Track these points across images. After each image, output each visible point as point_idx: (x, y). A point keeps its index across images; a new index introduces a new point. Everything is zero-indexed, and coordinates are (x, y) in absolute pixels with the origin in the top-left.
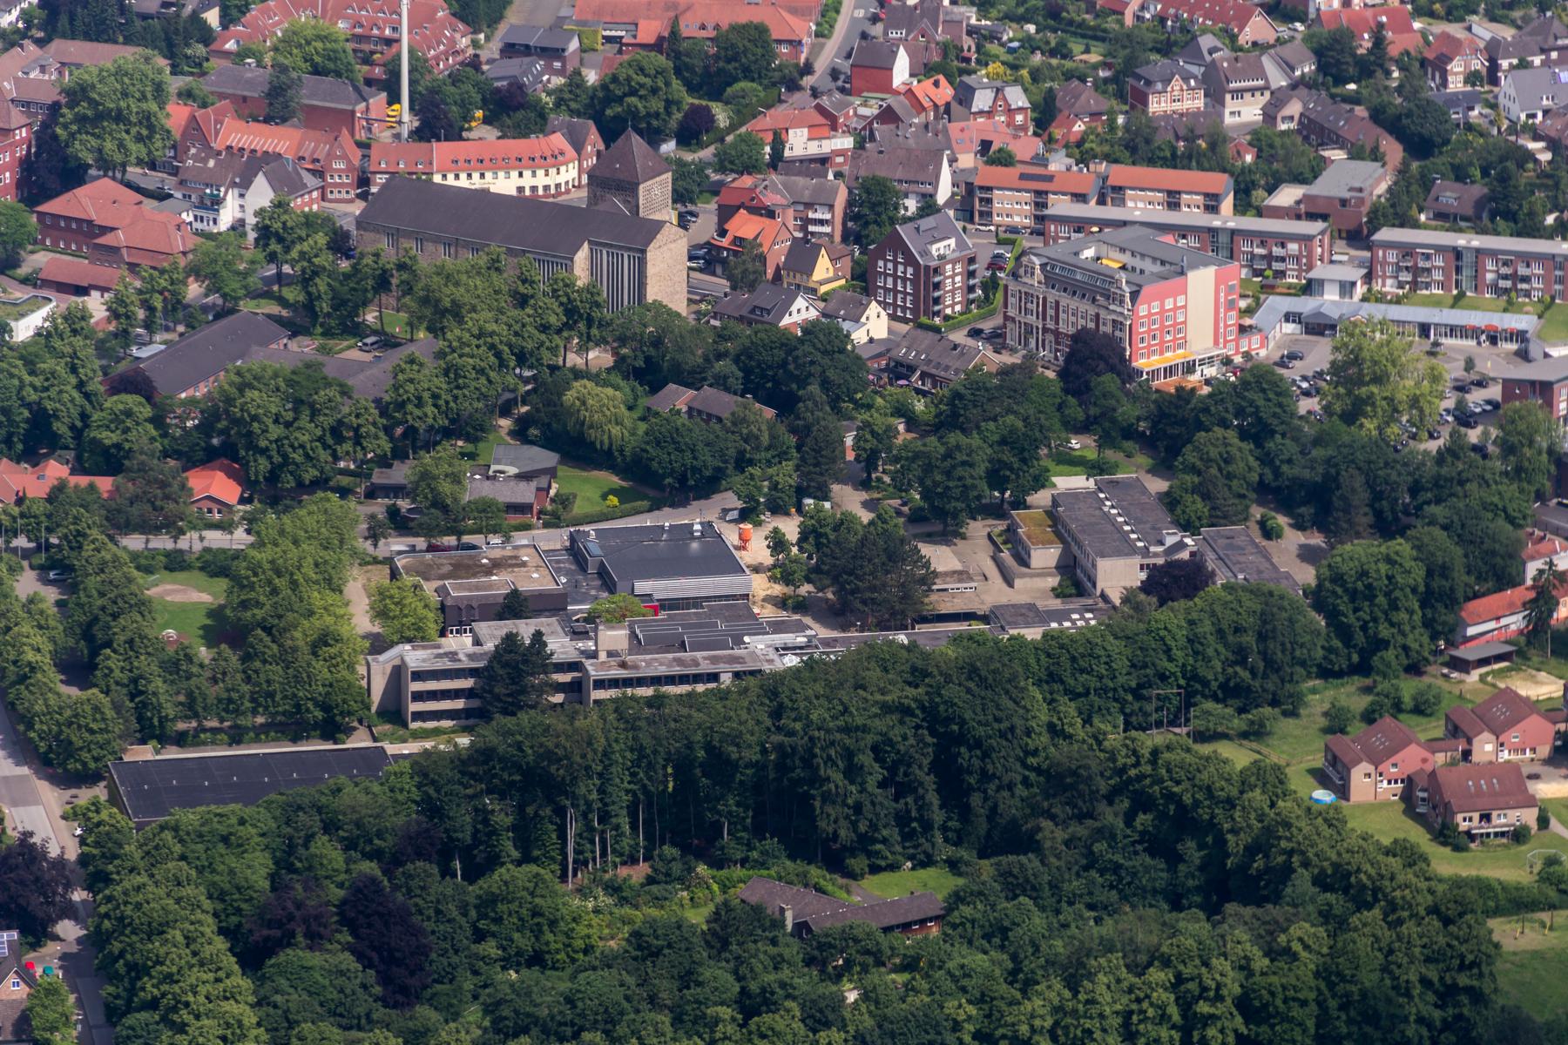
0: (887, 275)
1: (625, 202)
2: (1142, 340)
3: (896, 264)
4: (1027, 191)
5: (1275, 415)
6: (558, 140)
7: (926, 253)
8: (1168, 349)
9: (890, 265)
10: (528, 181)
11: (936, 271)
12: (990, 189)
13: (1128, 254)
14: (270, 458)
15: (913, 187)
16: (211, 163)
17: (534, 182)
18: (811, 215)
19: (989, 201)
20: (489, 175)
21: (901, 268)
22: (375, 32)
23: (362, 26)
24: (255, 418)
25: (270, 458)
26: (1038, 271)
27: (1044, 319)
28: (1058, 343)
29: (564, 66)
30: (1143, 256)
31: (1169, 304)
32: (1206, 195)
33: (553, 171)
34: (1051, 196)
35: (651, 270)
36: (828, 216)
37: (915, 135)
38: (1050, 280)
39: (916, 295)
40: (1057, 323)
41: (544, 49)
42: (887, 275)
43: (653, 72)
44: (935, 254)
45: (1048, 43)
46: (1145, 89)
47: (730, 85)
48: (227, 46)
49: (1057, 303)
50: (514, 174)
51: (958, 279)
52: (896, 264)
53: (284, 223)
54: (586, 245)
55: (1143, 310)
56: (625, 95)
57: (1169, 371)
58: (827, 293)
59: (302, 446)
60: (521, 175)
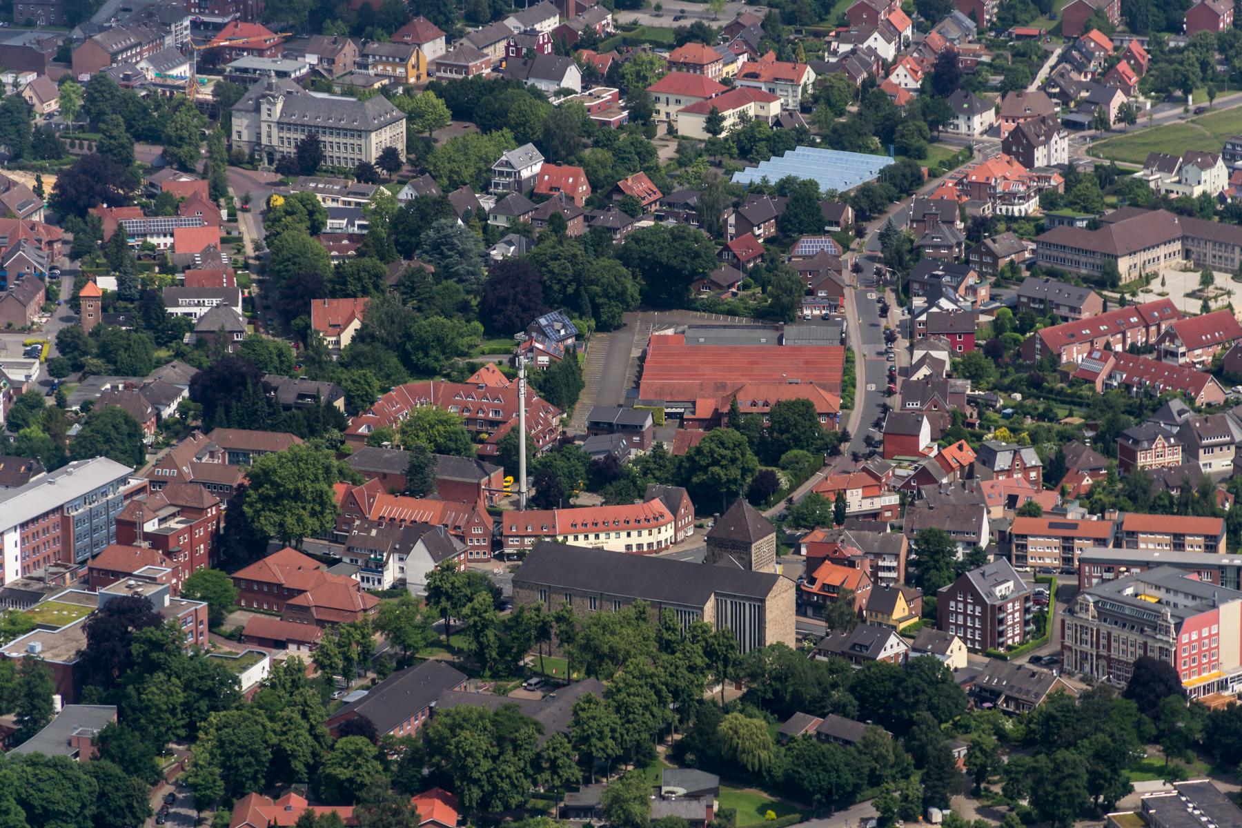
1: (740, 559)
3: (966, 604)
4: (1056, 538)
6: (657, 505)
7: (991, 594)
9: (961, 605)
10: (634, 540)
12: (1025, 537)
13: (1163, 591)
14: (481, 787)
15: (960, 537)
16: (374, 533)
17: (640, 540)
18: (880, 563)
19: (1024, 547)
20: (602, 536)
21: (970, 608)
22: (481, 415)
23: (469, 410)
24: (469, 754)
25: (481, 787)
26: (1092, 607)
27: (1098, 647)
28: (1109, 667)
29: (642, 440)
30: (1176, 592)
31: (1205, 633)
32: (1206, 537)
33: (655, 531)
35: (769, 616)
36: (895, 564)
37: (954, 492)
38: (1103, 615)
40: (1109, 650)
41: (624, 426)
43: (731, 445)
44: (998, 594)
45: (1036, 409)
46: (1133, 447)
47: (784, 452)
49: (1109, 634)
50: (623, 534)
51: (1017, 614)
52: (966, 604)
55: (1185, 639)
56: (708, 465)
57: (1207, 689)
58: (904, 629)
59: (509, 777)
60: (629, 535)
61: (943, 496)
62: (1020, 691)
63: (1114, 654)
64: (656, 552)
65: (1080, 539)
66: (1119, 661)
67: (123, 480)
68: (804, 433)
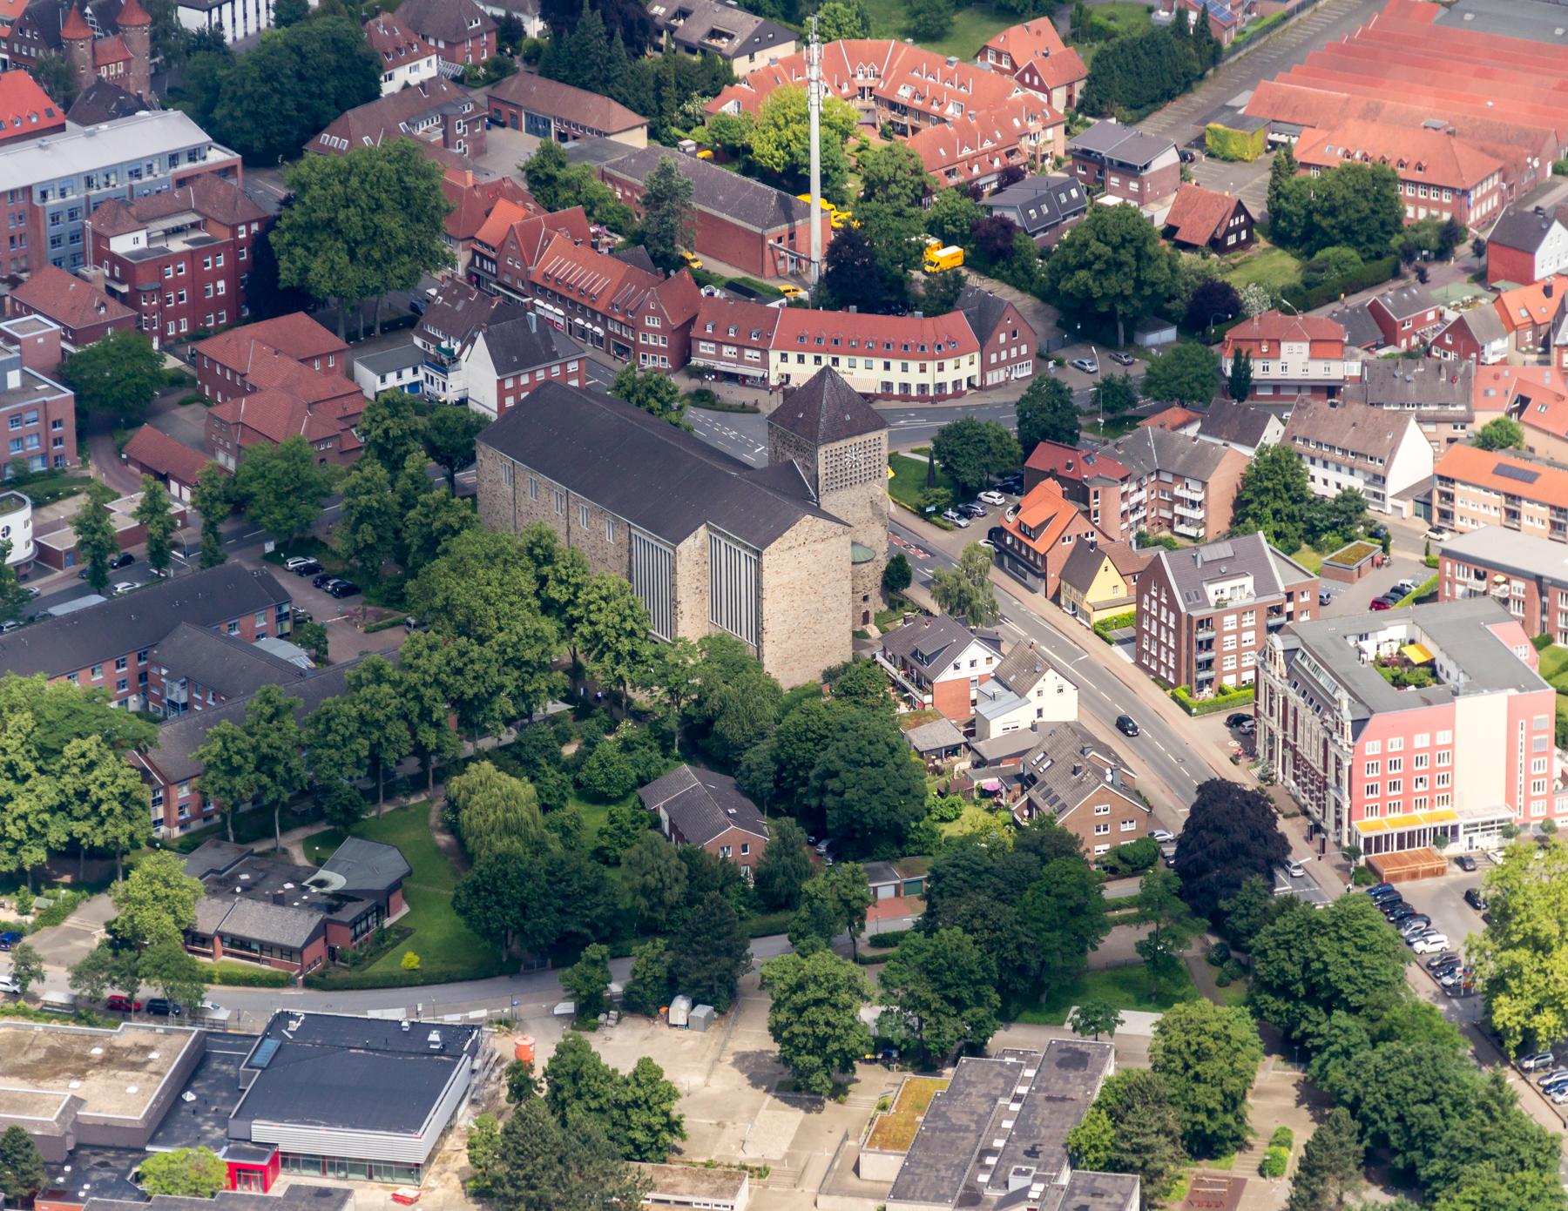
0: (1152, 617)
2: (1371, 790)
5: (1348, 979)
7: (1198, 597)
8: (1393, 808)
11: (1204, 623)
15: (1360, 462)
17: (905, 378)
19: (1449, 497)
22: (935, 108)
23: (923, 98)
26: (1280, 659)
34: (1524, 504)
35: (768, 578)
36: (1199, 497)
37: (1421, 378)
39: (1177, 651)
41: (1121, 164)
43: (1116, 240)
47: (1325, 246)
48: (725, 108)
50: (878, 363)
51: (1249, 636)
53: (386, 431)
54: (702, 531)
55: (1372, 747)
58: (1103, 624)
60: (887, 366)
61: (1398, 382)
64: (933, 400)
65: (1530, 501)
67: (193, 154)
68: (1361, 221)
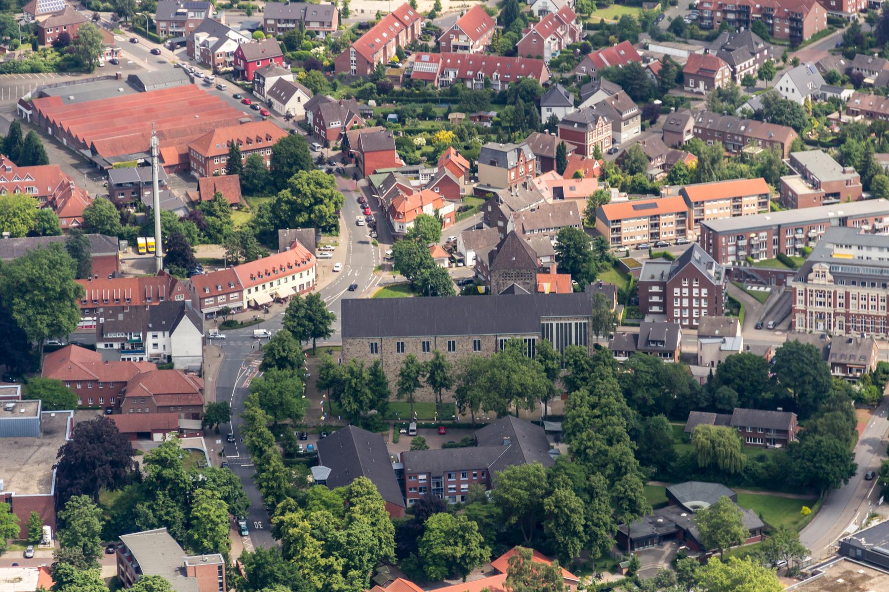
1: (524, 284)
3: (691, 288)
4: (645, 218)
9: (686, 291)
10: (298, 282)
12: (619, 221)
13: (854, 248)
14: (580, 538)
16: (121, 317)
19: (618, 230)
20: (275, 283)
21: (695, 291)
24: (573, 511)
25: (580, 538)
27: (835, 306)
28: (847, 321)
30: (869, 247)
38: (838, 279)
40: (847, 306)
42: (681, 297)
45: (414, 111)
46: (582, 130)
49: (847, 294)
50: (290, 278)
52: (691, 288)
56: (311, 205)
59: (605, 524)
62: (842, 356)
63: (853, 310)
65: (665, 215)
66: (859, 315)
